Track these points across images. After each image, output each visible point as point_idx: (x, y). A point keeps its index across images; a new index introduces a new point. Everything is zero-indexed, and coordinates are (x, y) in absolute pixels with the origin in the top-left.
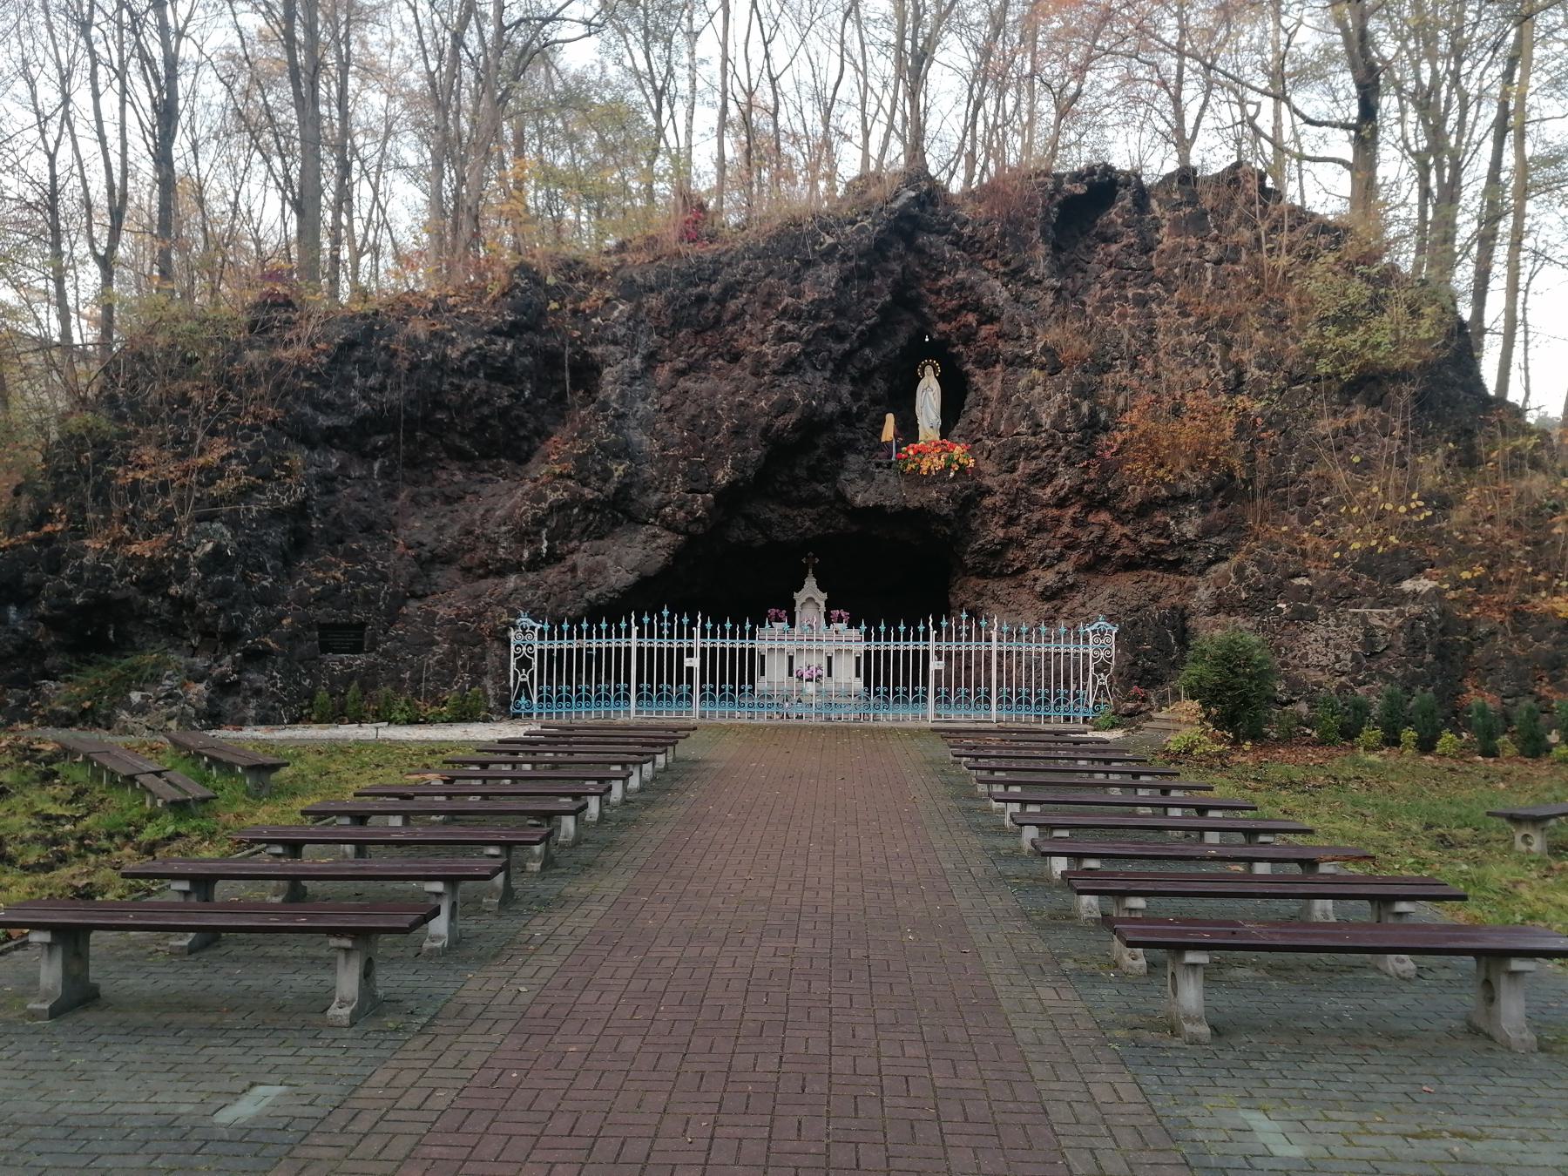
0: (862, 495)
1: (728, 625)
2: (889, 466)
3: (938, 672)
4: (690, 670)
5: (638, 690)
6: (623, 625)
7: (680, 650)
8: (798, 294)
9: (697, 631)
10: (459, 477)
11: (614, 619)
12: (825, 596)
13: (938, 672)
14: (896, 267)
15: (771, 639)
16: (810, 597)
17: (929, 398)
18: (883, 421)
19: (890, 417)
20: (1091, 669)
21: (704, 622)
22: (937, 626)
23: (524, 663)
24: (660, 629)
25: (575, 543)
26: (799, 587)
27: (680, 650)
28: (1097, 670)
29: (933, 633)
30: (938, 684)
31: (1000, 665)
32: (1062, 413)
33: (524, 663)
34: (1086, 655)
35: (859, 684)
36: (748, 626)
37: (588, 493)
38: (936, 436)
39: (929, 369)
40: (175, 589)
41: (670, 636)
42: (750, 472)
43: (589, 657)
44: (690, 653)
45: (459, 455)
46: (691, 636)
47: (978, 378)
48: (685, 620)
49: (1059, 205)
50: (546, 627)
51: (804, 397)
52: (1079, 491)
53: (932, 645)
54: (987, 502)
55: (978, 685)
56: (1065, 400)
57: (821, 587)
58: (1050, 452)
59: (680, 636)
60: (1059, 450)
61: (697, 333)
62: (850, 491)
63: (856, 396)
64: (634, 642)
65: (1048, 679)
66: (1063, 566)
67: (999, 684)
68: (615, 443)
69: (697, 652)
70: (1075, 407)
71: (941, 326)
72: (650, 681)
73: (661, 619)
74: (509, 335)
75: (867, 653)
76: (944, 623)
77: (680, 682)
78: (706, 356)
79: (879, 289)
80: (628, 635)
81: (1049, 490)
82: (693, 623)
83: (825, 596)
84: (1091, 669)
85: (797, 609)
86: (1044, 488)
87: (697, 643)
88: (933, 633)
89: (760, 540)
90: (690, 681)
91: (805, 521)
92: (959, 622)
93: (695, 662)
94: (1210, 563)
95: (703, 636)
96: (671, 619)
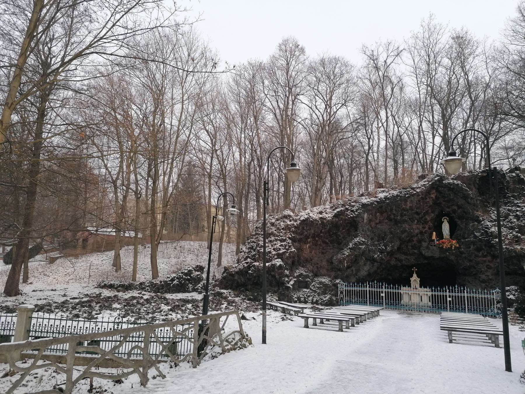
0: (428, 253)
2: (435, 246)
3: (450, 301)
4: (382, 297)
5: (369, 301)
7: (380, 292)
8: (406, 205)
9: (384, 287)
11: (363, 283)
12: (419, 279)
13: (450, 301)
14: (433, 196)
15: (404, 290)
16: (415, 279)
17: (446, 228)
18: (432, 234)
19: (434, 233)
22: (449, 289)
23: (342, 293)
24: (374, 286)
26: (412, 276)
27: (380, 292)
30: (450, 304)
33: (342, 293)
34: (493, 299)
35: (430, 304)
38: (448, 237)
40: (272, 273)
41: (377, 288)
42: (396, 248)
44: (382, 293)
46: (382, 288)
47: (459, 222)
48: (381, 284)
49: (479, 178)
51: (409, 229)
53: (448, 294)
54: (464, 255)
55: (462, 305)
57: (418, 277)
59: (379, 288)
62: (423, 252)
63: (424, 228)
65: (482, 304)
66: (488, 274)
67: (468, 305)
69: (384, 292)
71: (448, 210)
72: (372, 299)
73: (374, 284)
75: (432, 295)
76: (451, 288)
77: (380, 299)
78: (383, 219)
79: (429, 202)
80: (366, 287)
82: (382, 285)
83: (419, 279)
84: (495, 302)
89: (399, 264)
90: (382, 299)
91: (412, 260)
93: (384, 295)
95: (385, 288)
96: (377, 284)
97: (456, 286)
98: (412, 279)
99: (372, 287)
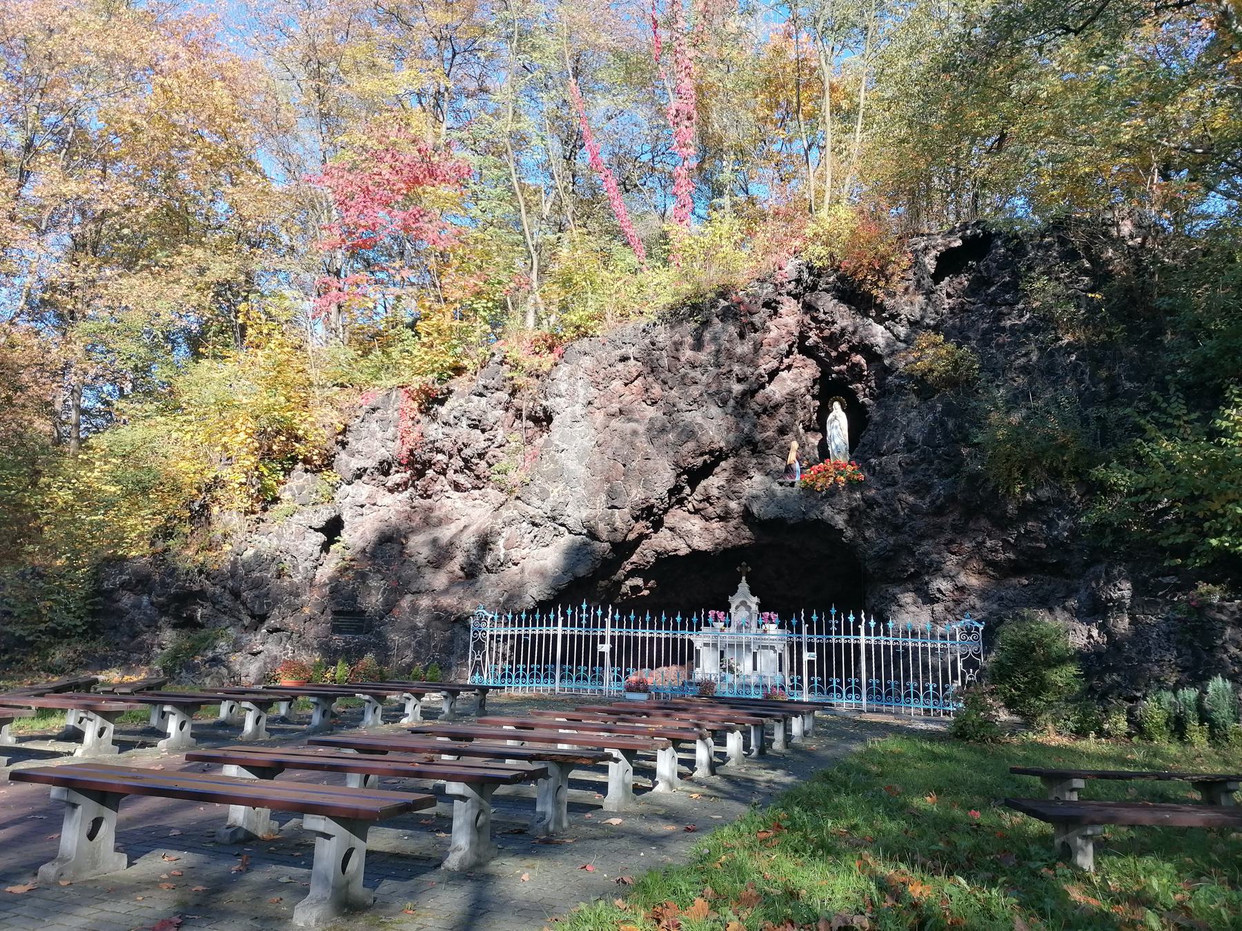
1: (632, 617)
4: (602, 654)
5: (563, 670)
6: (552, 616)
9: (608, 621)
10: (459, 504)
13: (810, 663)
20: (960, 665)
21: (614, 614)
24: (580, 619)
25: (527, 550)
27: (595, 637)
28: (965, 664)
29: (805, 627)
30: (811, 674)
31: (868, 659)
32: (932, 431)
36: (648, 618)
37: (531, 511)
39: (836, 405)
41: (588, 626)
43: (526, 641)
44: (603, 642)
45: (457, 487)
46: (603, 626)
48: (599, 612)
50: (496, 617)
52: (952, 498)
56: (935, 418)
58: (924, 466)
60: (931, 463)
61: (626, 385)
64: (560, 630)
68: (555, 471)
69: (608, 640)
70: (943, 424)
74: (481, 395)
80: (556, 624)
81: (928, 500)
82: (605, 615)
85: (732, 610)
86: (923, 498)
87: (608, 632)
88: (805, 627)
89: (684, 551)
90: (602, 664)
92: (829, 617)
93: (605, 648)
94: (1088, 565)
95: (613, 626)
97: (833, 611)
98: (734, 601)
99: (573, 625)
